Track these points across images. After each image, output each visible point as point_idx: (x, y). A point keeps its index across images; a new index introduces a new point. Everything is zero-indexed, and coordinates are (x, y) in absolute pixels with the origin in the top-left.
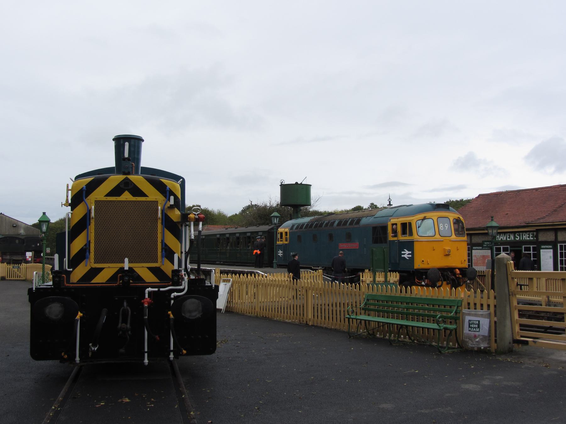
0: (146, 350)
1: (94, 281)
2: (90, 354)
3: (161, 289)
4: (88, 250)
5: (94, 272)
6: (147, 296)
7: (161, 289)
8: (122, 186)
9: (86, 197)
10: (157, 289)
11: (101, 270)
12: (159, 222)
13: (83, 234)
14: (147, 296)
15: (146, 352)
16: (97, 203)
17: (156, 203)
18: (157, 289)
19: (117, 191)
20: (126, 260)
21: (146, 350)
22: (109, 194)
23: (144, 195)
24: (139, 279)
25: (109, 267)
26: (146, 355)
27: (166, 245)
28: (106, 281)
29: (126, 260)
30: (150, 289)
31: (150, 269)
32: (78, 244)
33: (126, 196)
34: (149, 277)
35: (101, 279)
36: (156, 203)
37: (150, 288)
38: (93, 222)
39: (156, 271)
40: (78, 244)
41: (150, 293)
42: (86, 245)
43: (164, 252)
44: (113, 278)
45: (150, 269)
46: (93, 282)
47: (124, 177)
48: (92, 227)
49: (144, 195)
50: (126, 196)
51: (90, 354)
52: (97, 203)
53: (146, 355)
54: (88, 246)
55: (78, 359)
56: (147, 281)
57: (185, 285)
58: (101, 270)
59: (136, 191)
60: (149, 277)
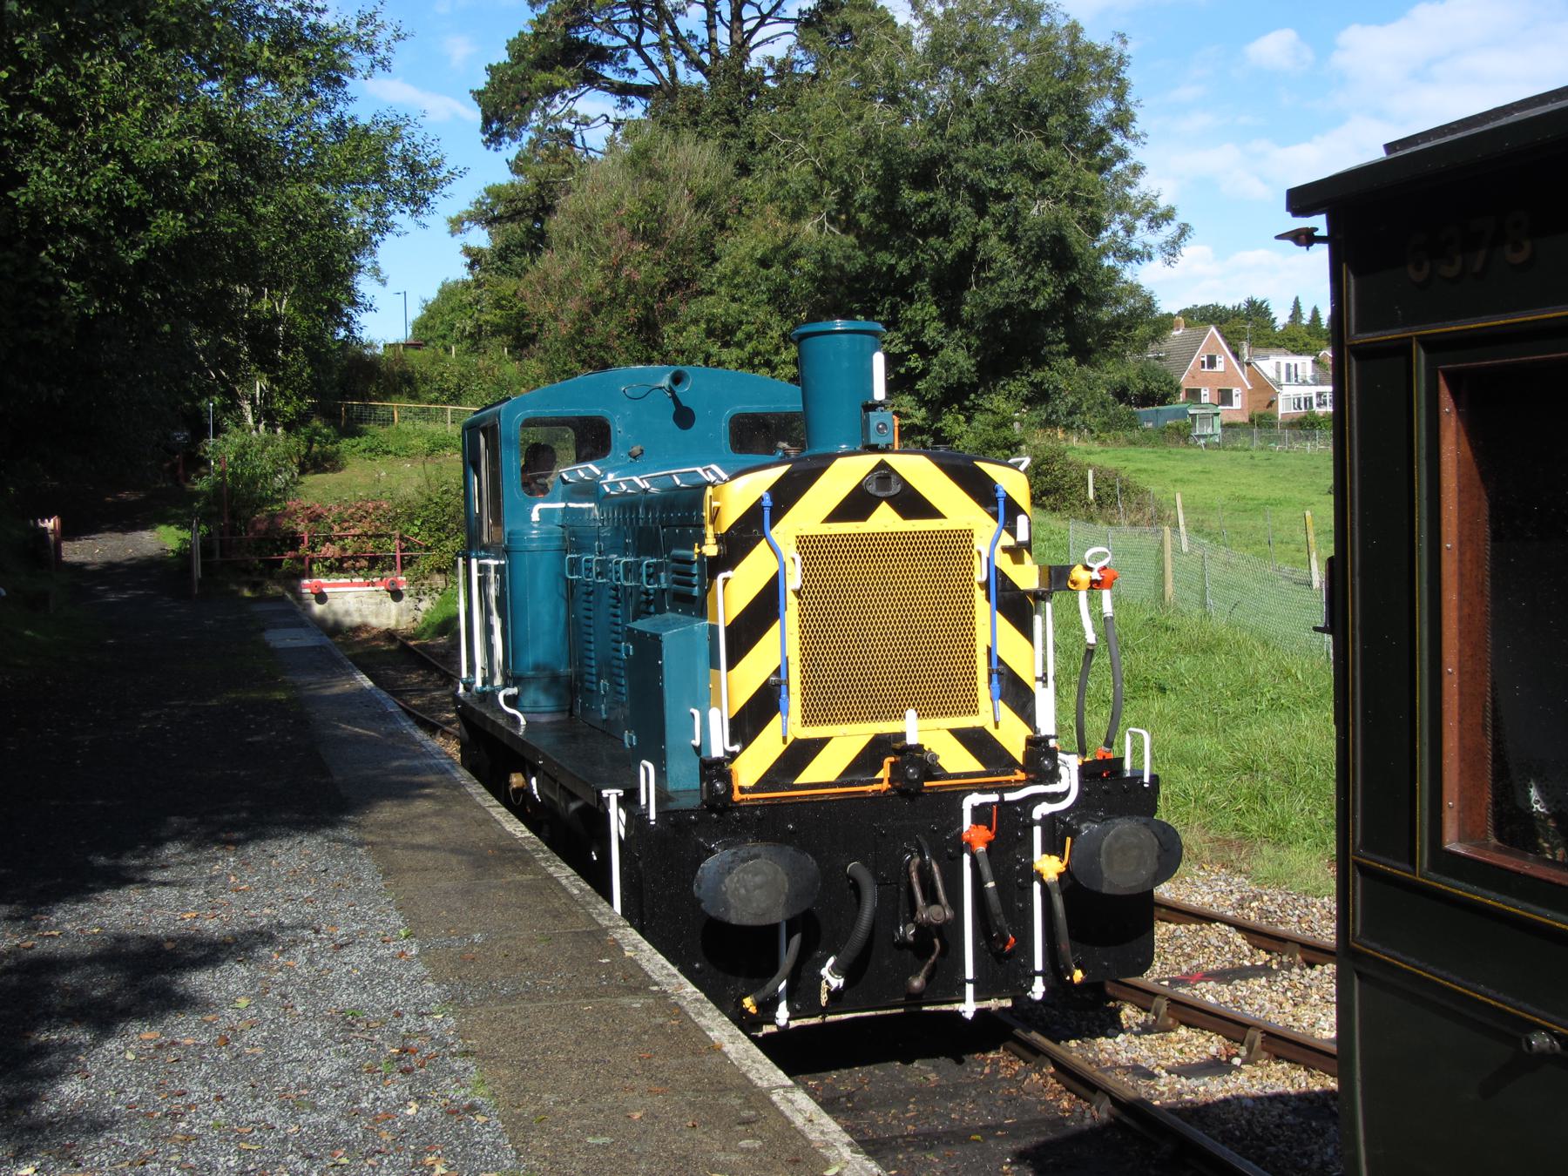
0: (969, 974)
1: (806, 777)
2: (824, 998)
3: (1009, 797)
4: (784, 688)
5: (800, 753)
7: (1009, 797)
8: (872, 489)
9: (773, 523)
11: (821, 743)
15: (970, 982)
16: (806, 545)
17: (969, 534)
18: (994, 798)
19: (856, 505)
21: (969, 974)
22: (837, 515)
23: (930, 512)
25: (845, 735)
27: (1000, 661)
28: (842, 775)
30: (974, 799)
31: (961, 735)
33: (885, 519)
35: (823, 769)
36: (969, 534)
37: (975, 795)
39: (976, 741)
41: (980, 813)
42: (777, 672)
43: (995, 682)
46: (803, 779)
50: (885, 519)
51: (824, 998)
52: (806, 545)
54: (783, 677)
56: (950, 769)
58: (821, 743)
59: (913, 504)
60: (957, 760)
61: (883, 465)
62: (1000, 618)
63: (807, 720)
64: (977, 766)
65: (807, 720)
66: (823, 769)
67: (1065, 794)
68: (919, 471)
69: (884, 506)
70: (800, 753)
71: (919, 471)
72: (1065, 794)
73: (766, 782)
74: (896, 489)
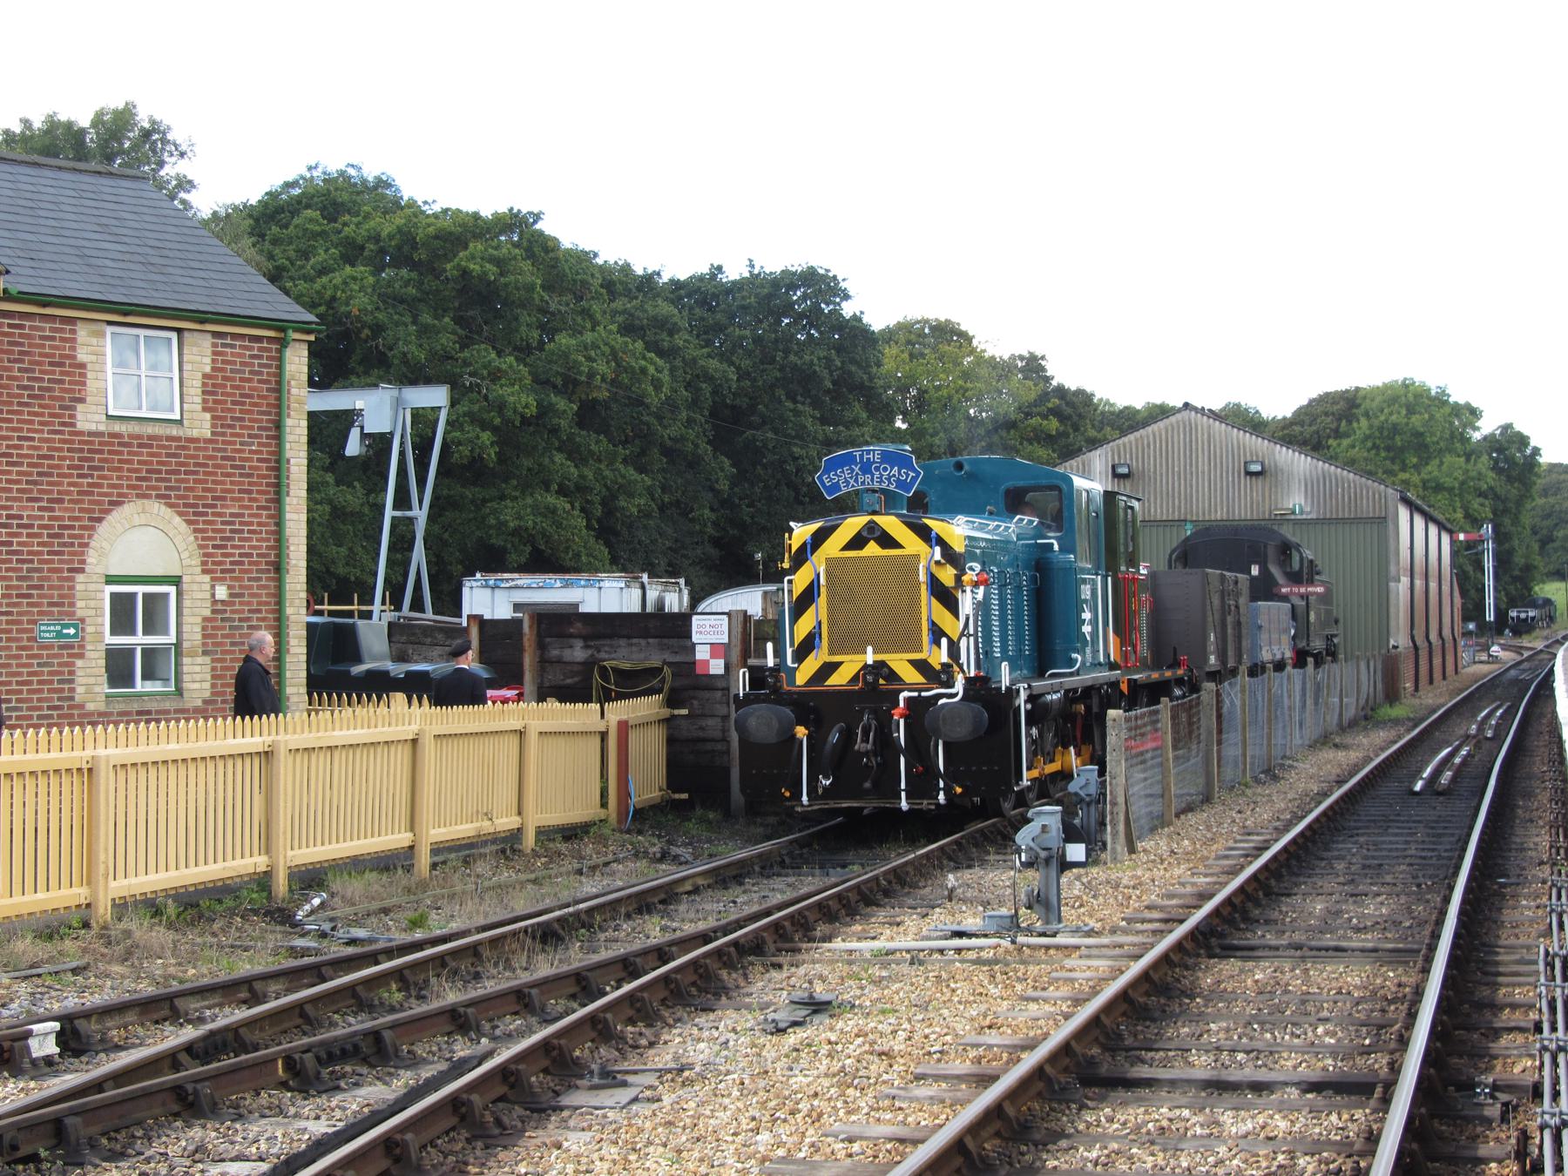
0: (903, 786)
1: (831, 681)
2: (820, 791)
3: (923, 694)
5: (829, 669)
6: (902, 704)
7: (923, 694)
8: (865, 534)
10: (916, 694)
12: (923, 587)
13: (812, 609)
14: (902, 704)
16: (830, 562)
17: (917, 557)
18: (916, 694)
19: (857, 542)
20: (870, 649)
21: (903, 786)
22: (847, 547)
23: (898, 545)
24: (893, 676)
26: (903, 794)
29: (870, 649)
32: (805, 625)
33: (872, 549)
34: (911, 675)
35: (839, 679)
36: (917, 557)
38: (823, 590)
39: (922, 666)
40: (805, 625)
44: (855, 679)
45: (911, 662)
47: (868, 518)
48: (822, 601)
49: (898, 545)
50: (872, 549)
51: (820, 791)
52: (830, 562)
53: (903, 794)
55: (805, 798)
57: (959, 686)
59: (887, 541)
60: (911, 675)
61: (872, 522)
62: (934, 600)
63: (831, 653)
64: (924, 681)
65: (831, 653)
66: (839, 679)
67: (956, 695)
68: (890, 523)
69: (872, 543)
70: (829, 669)
71: (890, 523)
72: (956, 695)
73: (812, 681)
74: (877, 534)
